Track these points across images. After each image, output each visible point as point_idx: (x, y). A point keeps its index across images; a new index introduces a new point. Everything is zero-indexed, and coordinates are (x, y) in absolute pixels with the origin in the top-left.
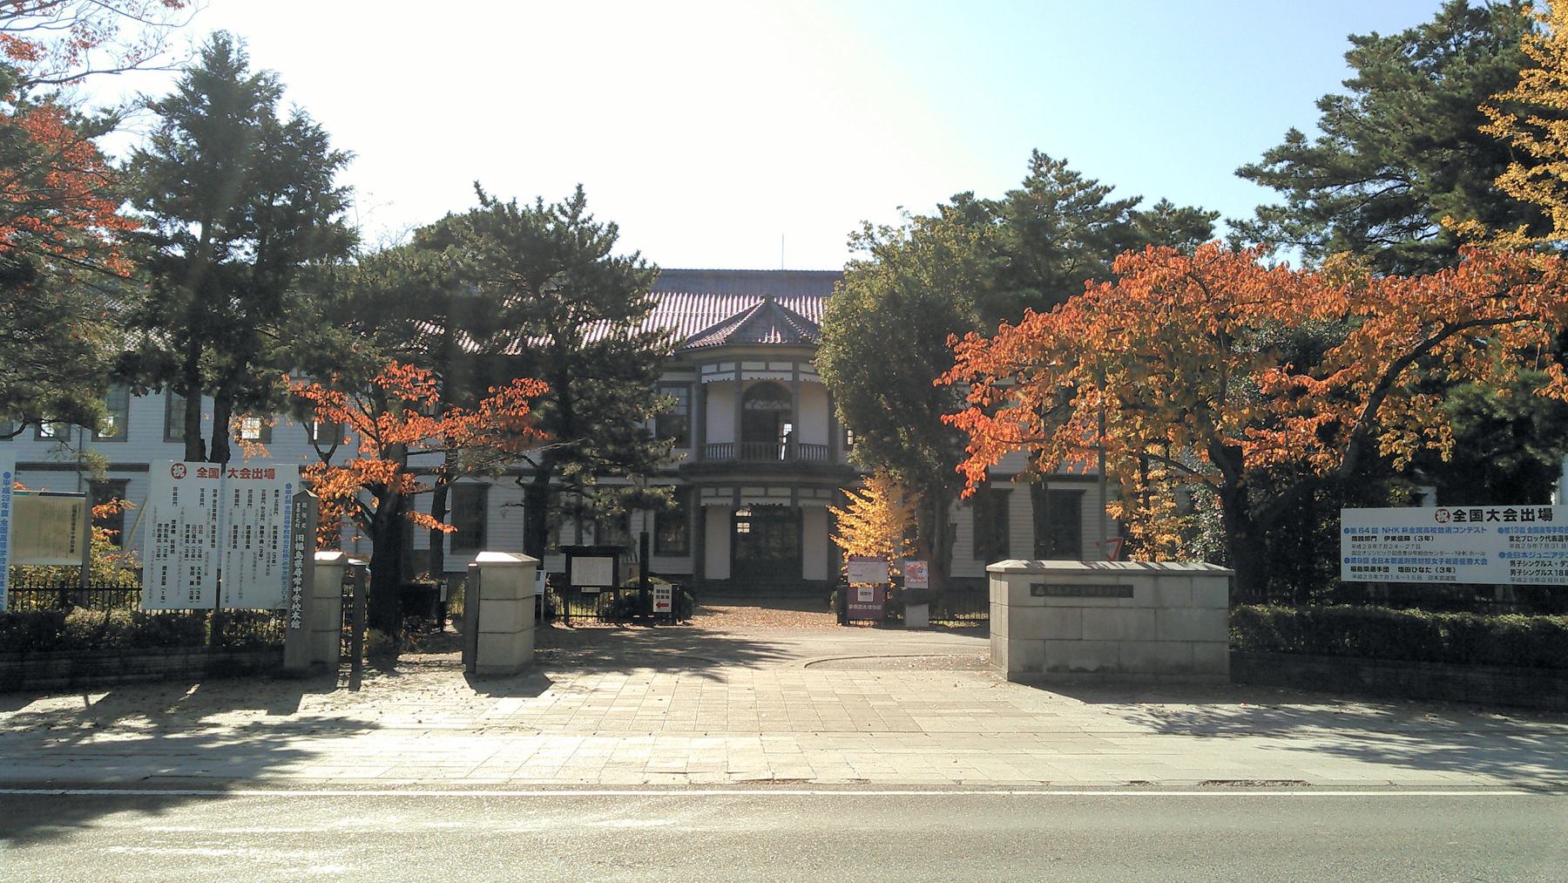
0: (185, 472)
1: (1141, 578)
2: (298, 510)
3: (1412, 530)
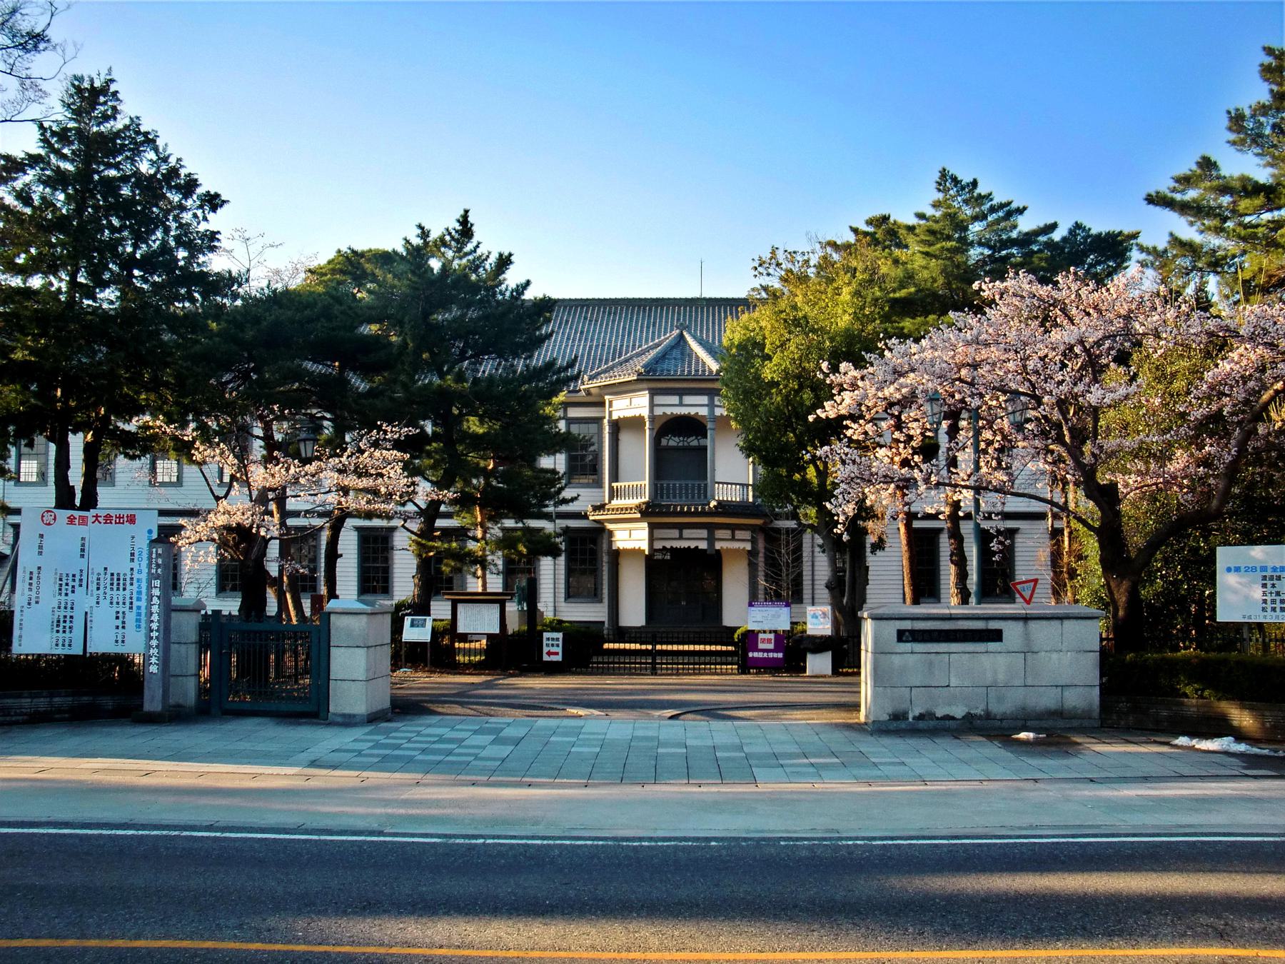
0: (55, 519)
1: (1010, 622)
2: (154, 556)
3: (38, 593)
